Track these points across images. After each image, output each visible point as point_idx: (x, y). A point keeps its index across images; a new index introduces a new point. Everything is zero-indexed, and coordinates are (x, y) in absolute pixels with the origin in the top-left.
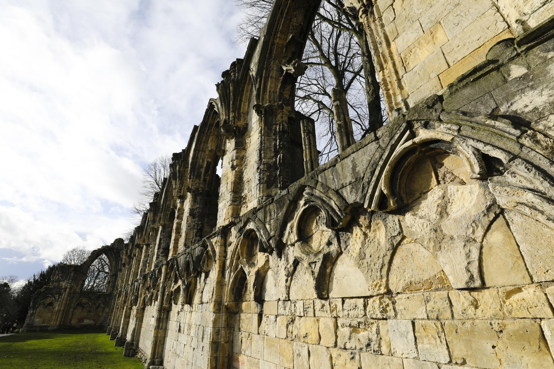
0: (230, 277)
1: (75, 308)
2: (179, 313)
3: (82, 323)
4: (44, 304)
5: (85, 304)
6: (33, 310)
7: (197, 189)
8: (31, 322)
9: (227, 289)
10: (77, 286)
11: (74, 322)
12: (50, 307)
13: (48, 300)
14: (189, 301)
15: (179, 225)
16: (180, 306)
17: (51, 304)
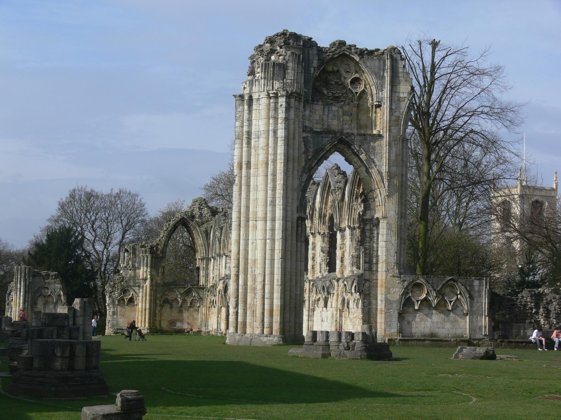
0: (340, 299)
1: (162, 306)
2: (321, 312)
3: (175, 327)
4: (124, 300)
5: (173, 301)
6: (114, 308)
7: (324, 233)
8: (115, 322)
9: (339, 303)
10: (158, 276)
11: (165, 325)
12: (132, 304)
13: (126, 294)
14: (326, 306)
15: (314, 255)
16: (321, 309)
17: (131, 301)
